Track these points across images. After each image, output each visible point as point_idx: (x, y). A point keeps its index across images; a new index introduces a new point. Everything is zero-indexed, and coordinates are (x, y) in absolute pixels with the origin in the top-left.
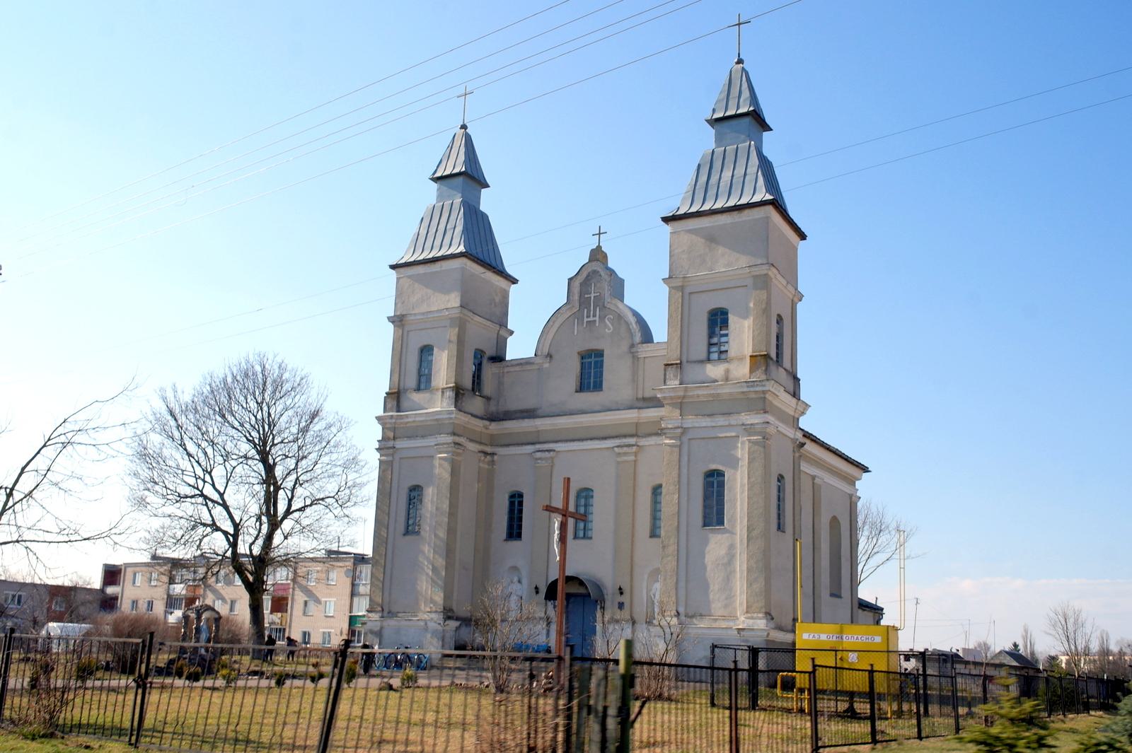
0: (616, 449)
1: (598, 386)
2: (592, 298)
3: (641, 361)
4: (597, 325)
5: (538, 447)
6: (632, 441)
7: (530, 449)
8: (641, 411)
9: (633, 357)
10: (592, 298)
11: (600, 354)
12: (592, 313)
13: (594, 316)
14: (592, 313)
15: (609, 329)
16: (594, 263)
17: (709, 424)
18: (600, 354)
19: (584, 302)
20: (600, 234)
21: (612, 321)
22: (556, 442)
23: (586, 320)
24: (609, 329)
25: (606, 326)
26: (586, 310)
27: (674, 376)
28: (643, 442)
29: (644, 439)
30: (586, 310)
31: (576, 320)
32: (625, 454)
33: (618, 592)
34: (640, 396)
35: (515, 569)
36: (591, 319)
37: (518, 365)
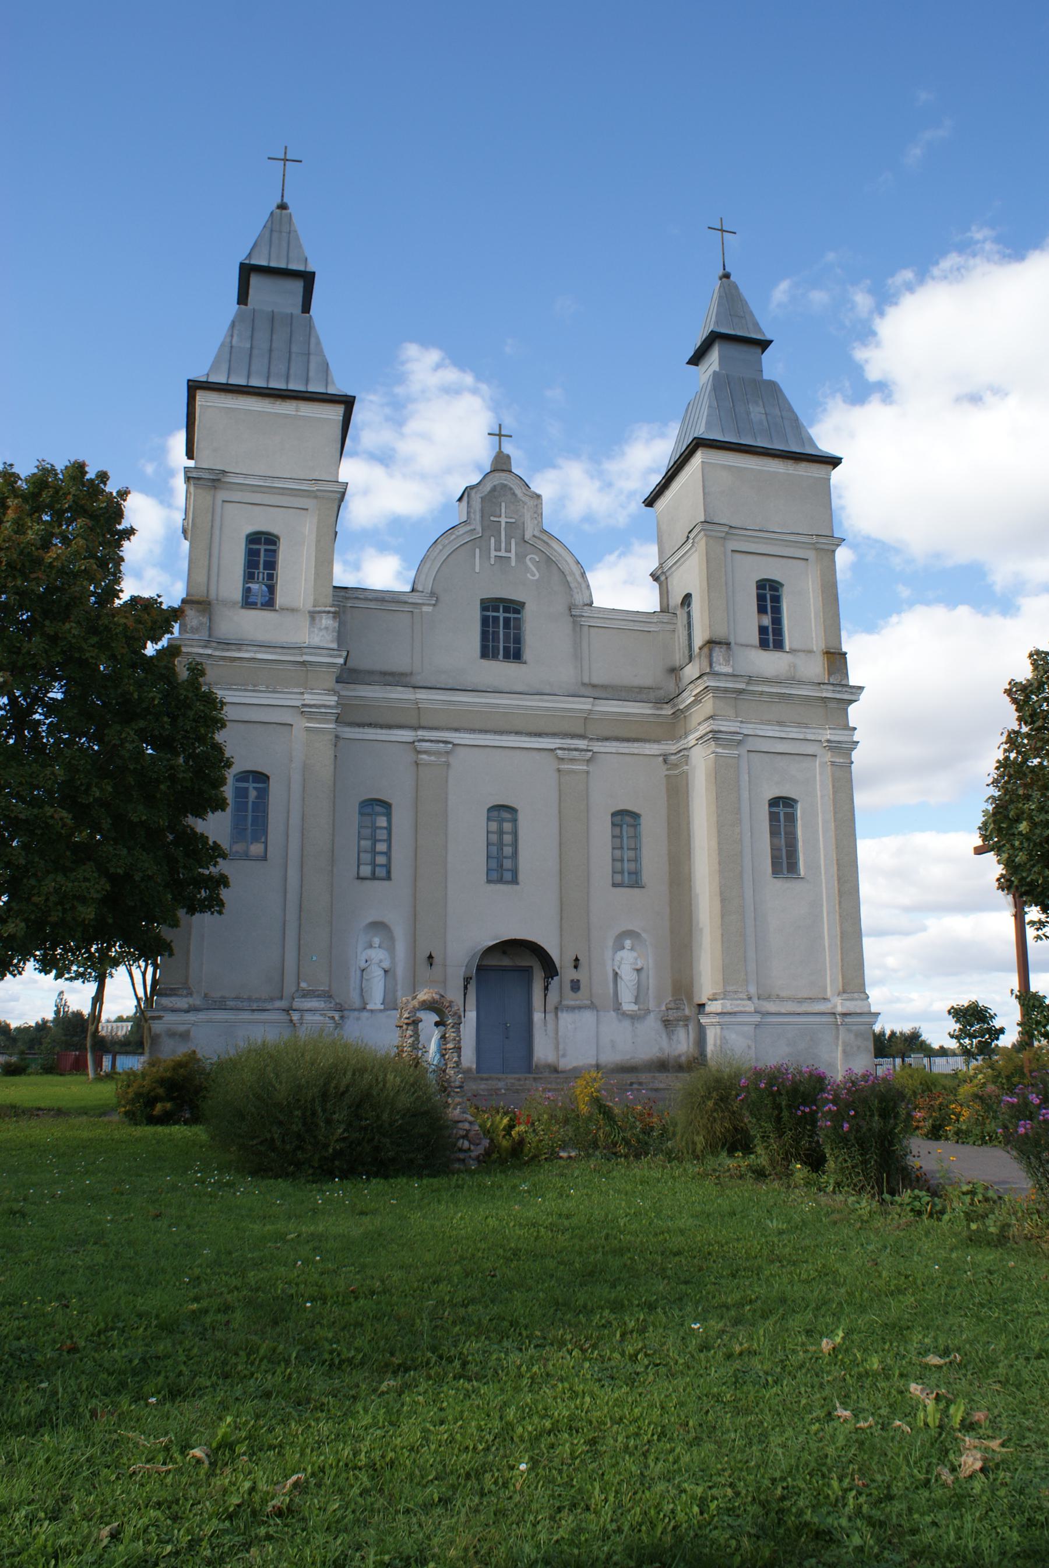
0: (559, 752)
1: (515, 655)
2: (503, 525)
3: (585, 629)
4: (513, 564)
5: (420, 733)
6: (582, 744)
7: (407, 735)
8: (597, 702)
9: (574, 622)
10: (503, 525)
11: (514, 607)
12: (503, 545)
13: (508, 551)
14: (503, 545)
15: (534, 575)
16: (497, 474)
17: (777, 734)
18: (514, 607)
19: (490, 527)
20: (500, 435)
21: (537, 564)
22: (457, 730)
23: (493, 553)
24: (534, 575)
25: (527, 570)
26: (493, 540)
27: (724, 659)
28: (597, 747)
29: (600, 744)
30: (493, 540)
31: (477, 550)
32: (572, 760)
33: (573, 964)
34: (586, 680)
35: (379, 926)
36: (503, 554)
37: (376, 600)
